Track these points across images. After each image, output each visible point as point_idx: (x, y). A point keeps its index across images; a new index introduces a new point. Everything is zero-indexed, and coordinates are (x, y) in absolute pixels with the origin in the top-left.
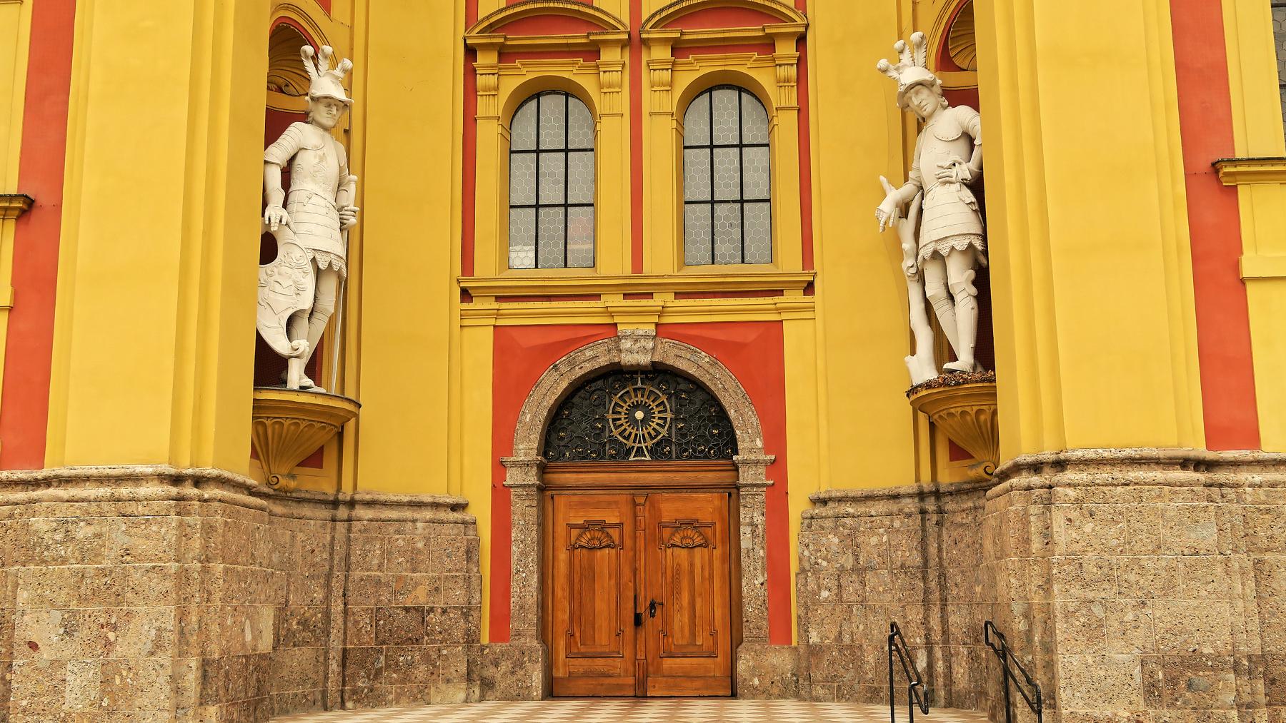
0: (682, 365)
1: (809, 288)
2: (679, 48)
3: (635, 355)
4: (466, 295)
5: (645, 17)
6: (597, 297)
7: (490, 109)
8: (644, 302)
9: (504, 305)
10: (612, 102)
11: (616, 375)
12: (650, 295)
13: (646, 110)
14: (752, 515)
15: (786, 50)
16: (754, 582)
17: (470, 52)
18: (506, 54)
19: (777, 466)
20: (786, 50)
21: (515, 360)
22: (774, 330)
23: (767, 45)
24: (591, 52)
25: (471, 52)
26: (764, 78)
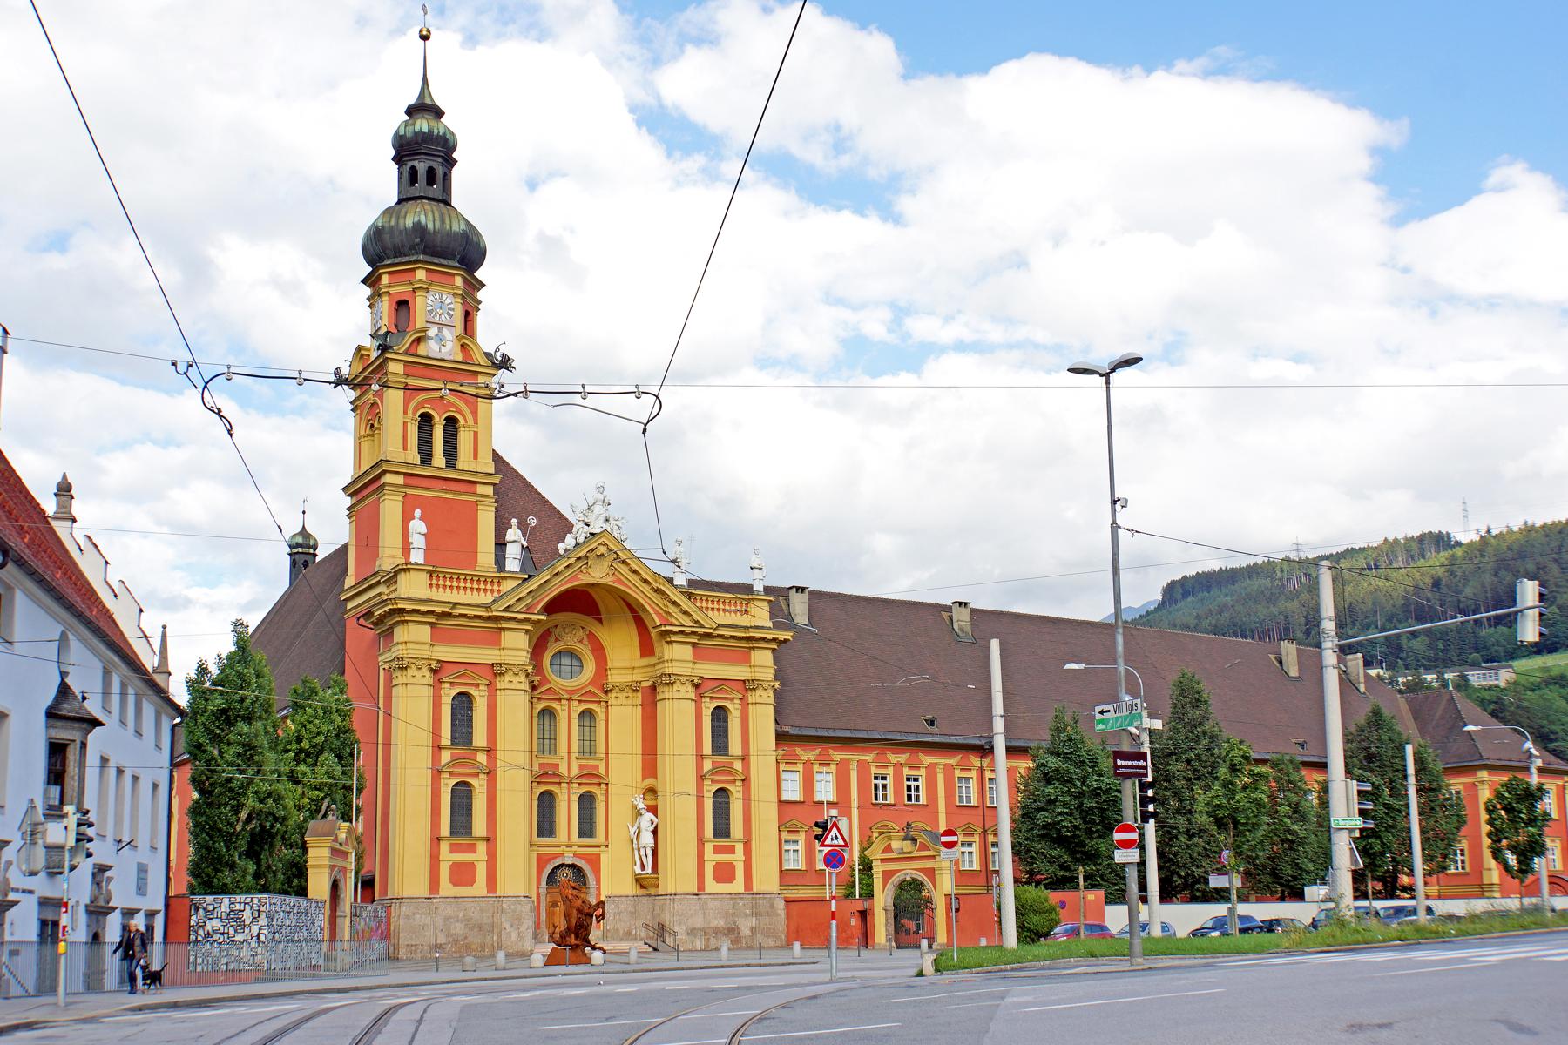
7: (536, 797)
11: (562, 865)
19: (599, 889)
21: (542, 861)
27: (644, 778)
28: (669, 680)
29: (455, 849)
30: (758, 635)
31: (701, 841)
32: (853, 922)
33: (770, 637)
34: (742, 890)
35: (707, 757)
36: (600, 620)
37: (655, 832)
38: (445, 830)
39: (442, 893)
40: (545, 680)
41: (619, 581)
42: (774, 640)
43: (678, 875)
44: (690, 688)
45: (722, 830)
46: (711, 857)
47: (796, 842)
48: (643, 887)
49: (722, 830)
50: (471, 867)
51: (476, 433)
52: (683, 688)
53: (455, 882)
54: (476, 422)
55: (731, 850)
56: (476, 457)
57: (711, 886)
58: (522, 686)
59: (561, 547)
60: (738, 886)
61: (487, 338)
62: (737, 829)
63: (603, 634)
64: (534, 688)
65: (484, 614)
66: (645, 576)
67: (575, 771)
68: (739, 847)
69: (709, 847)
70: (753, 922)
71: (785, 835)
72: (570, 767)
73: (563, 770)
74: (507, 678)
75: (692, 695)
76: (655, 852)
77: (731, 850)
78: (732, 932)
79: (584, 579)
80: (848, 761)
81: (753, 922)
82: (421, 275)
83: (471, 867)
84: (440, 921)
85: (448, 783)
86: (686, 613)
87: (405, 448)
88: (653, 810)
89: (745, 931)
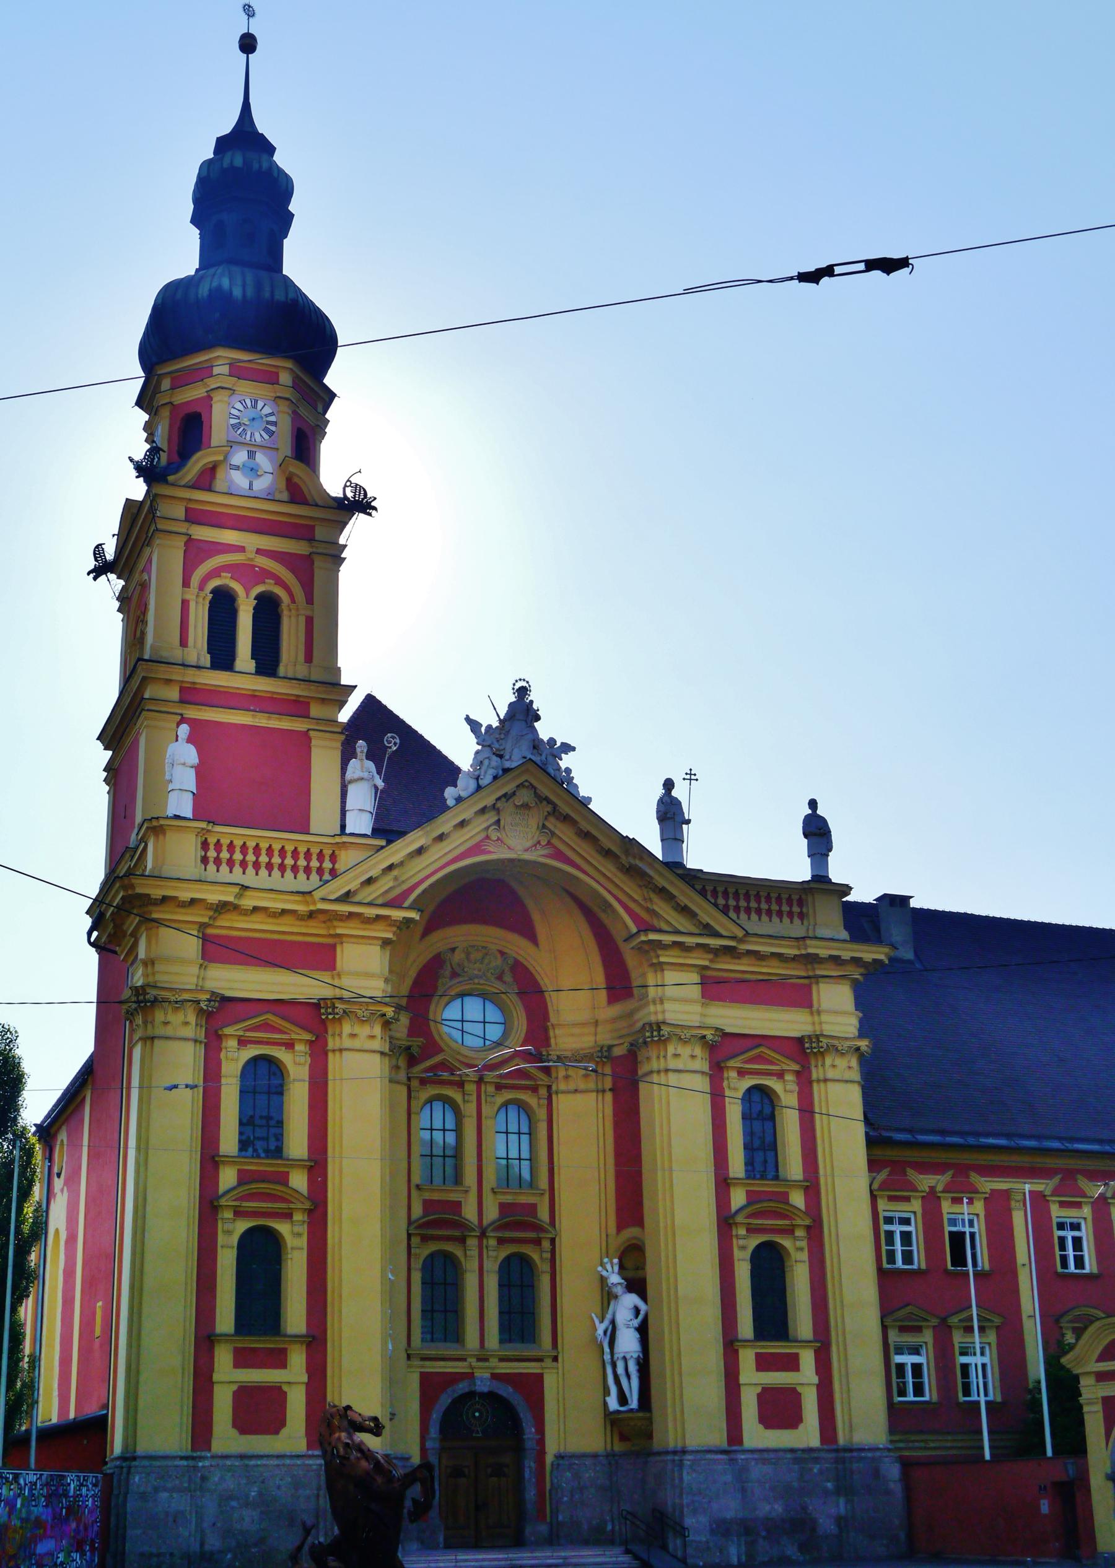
0: (500, 1392)
1: (555, 1359)
2: (501, 1241)
3: (482, 1387)
4: (409, 1357)
5: (485, 1223)
6: (465, 1360)
7: (417, 1264)
8: (487, 1364)
9: (428, 1363)
10: (471, 1266)
11: (471, 1395)
12: (486, 1360)
13: (485, 1268)
14: (530, 1464)
15: (546, 1244)
16: (531, 1494)
17: (409, 1236)
18: (425, 1239)
19: (541, 1442)
20: (546, 1244)
22: (540, 1377)
23: (537, 1242)
24: (462, 1240)
26: (535, 1257)
27: (620, 1228)
28: (656, 1034)
29: (242, 1359)
30: (823, 953)
31: (731, 1345)
32: (1045, 1507)
33: (846, 955)
34: (815, 1442)
35: (737, 1181)
36: (533, 938)
37: (643, 1330)
38: (225, 1319)
41: (559, 855)
42: (856, 961)
43: (693, 1413)
44: (698, 1051)
45: (772, 1319)
46: (752, 1379)
47: (916, 1351)
48: (623, 1438)
49: (772, 1319)
50: (275, 1396)
51: (309, 621)
53: (244, 1423)
54: (310, 600)
55: (791, 1363)
56: (309, 658)
57: (756, 1435)
58: (376, 1045)
59: (450, 793)
60: (808, 1434)
61: (332, 480)
62: (802, 1322)
63: (539, 961)
64: (412, 1061)
65: (301, 908)
66: (607, 844)
67: (492, 1213)
68: (807, 1359)
69: (747, 1358)
70: (841, 1506)
71: (894, 1336)
72: (479, 1207)
73: (470, 1212)
74: (347, 1028)
75: (701, 1063)
76: (644, 1366)
77: (791, 1363)
78: (799, 1525)
79: (498, 853)
80: (1006, 1194)
81: (841, 1506)
82: (221, 369)
84: (211, 1509)
85: (232, 1231)
86: (684, 910)
87: (184, 643)
88: (637, 1285)
89: (826, 1525)
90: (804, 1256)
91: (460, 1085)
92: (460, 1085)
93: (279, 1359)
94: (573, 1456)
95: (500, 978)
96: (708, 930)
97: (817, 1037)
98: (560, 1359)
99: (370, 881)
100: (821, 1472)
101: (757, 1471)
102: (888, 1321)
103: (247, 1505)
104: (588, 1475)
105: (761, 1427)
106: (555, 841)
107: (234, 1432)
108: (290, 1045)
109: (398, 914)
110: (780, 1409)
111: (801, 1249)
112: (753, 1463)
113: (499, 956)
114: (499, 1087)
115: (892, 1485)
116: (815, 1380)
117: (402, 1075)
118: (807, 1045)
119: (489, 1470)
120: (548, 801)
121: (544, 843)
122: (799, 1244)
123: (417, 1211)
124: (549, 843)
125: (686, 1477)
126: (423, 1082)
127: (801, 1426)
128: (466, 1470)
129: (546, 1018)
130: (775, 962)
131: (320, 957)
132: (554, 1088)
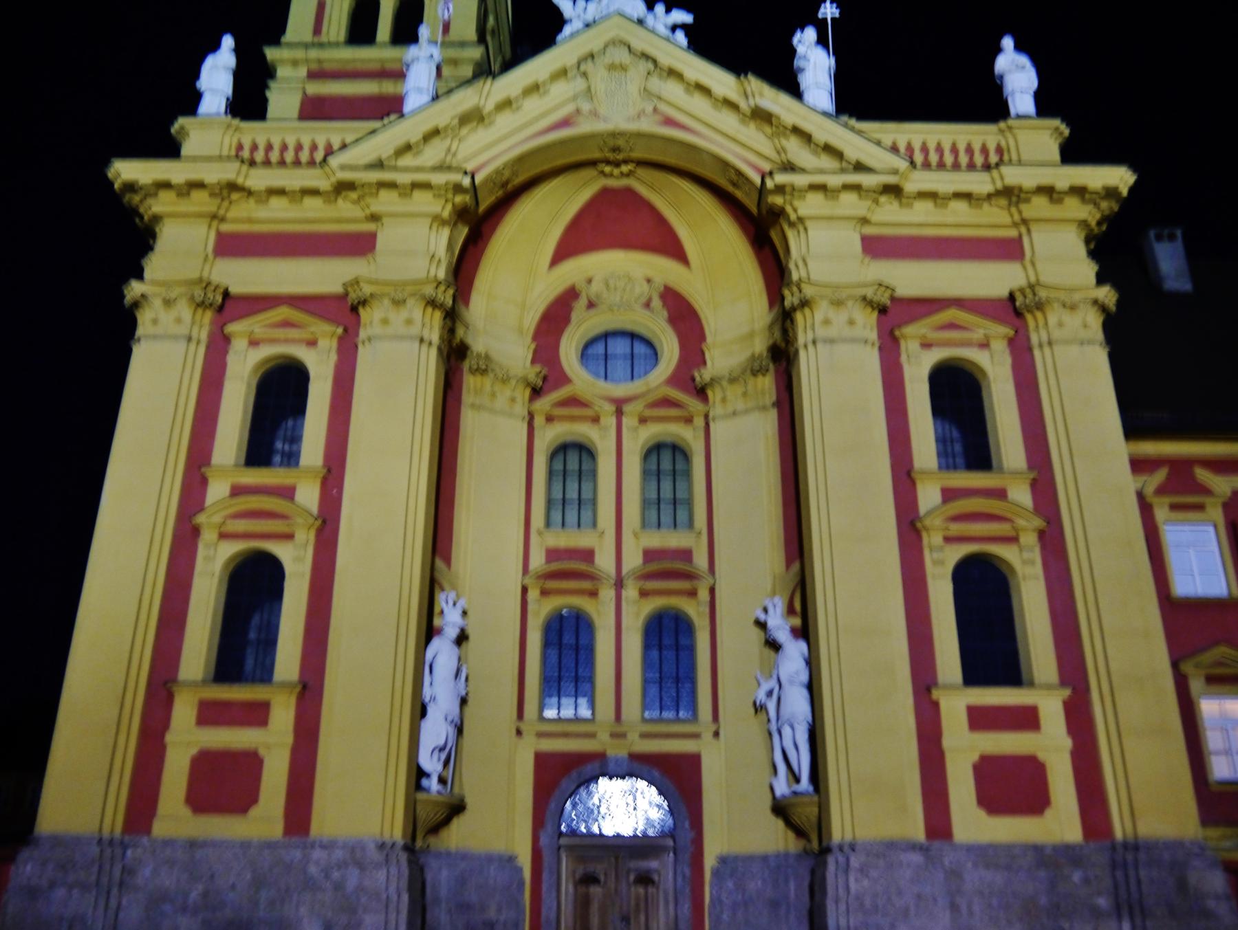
4: (519, 732)
5: (625, 570)
15: (704, 594)
18: (545, 593)
23: (693, 594)
24: (593, 594)
25: (525, 590)
39: (161, 828)
40: (564, 379)
42: (1079, 191)
50: (250, 763)
52: (839, 318)
57: (972, 823)
58: (415, 330)
60: (1061, 823)
67: (633, 560)
73: (605, 562)
77: (1027, 719)
83: (250, 763)
90: (1038, 569)
91: (596, 420)
92: (596, 420)
93: (257, 714)
94: (736, 858)
95: (647, 305)
96: (859, 167)
97: (1031, 287)
98: (722, 733)
99: (407, 148)
100: (1086, 881)
101: (974, 877)
102: (1187, 667)
103: (184, 909)
104: (754, 885)
105: (981, 814)
106: (663, 107)
107: (186, 812)
108: (312, 343)
109: (439, 179)
110: (1011, 786)
111: (1032, 563)
112: (969, 865)
113: (645, 283)
114: (643, 420)
115: (1211, 904)
116: (1068, 743)
117: (521, 409)
118: (1018, 304)
119: (632, 878)
120: (646, 56)
121: (649, 109)
122: (1026, 555)
123: (538, 561)
124: (655, 110)
125: (853, 886)
126: (550, 419)
127: (1049, 813)
128: (602, 878)
129: (702, 337)
130: (960, 206)
131: (360, 244)
132: (711, 415)
